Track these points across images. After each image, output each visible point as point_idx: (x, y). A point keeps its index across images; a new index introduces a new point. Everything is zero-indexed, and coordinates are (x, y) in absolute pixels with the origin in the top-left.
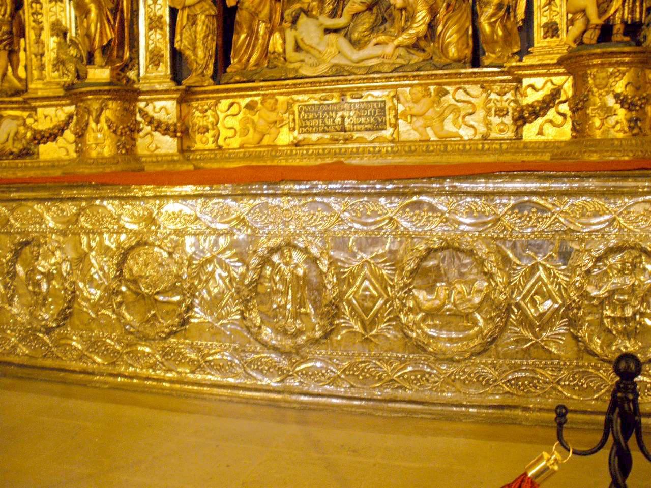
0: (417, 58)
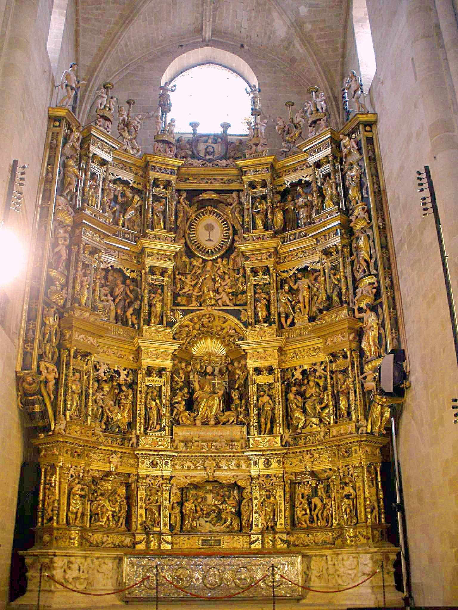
0: (228, 530)
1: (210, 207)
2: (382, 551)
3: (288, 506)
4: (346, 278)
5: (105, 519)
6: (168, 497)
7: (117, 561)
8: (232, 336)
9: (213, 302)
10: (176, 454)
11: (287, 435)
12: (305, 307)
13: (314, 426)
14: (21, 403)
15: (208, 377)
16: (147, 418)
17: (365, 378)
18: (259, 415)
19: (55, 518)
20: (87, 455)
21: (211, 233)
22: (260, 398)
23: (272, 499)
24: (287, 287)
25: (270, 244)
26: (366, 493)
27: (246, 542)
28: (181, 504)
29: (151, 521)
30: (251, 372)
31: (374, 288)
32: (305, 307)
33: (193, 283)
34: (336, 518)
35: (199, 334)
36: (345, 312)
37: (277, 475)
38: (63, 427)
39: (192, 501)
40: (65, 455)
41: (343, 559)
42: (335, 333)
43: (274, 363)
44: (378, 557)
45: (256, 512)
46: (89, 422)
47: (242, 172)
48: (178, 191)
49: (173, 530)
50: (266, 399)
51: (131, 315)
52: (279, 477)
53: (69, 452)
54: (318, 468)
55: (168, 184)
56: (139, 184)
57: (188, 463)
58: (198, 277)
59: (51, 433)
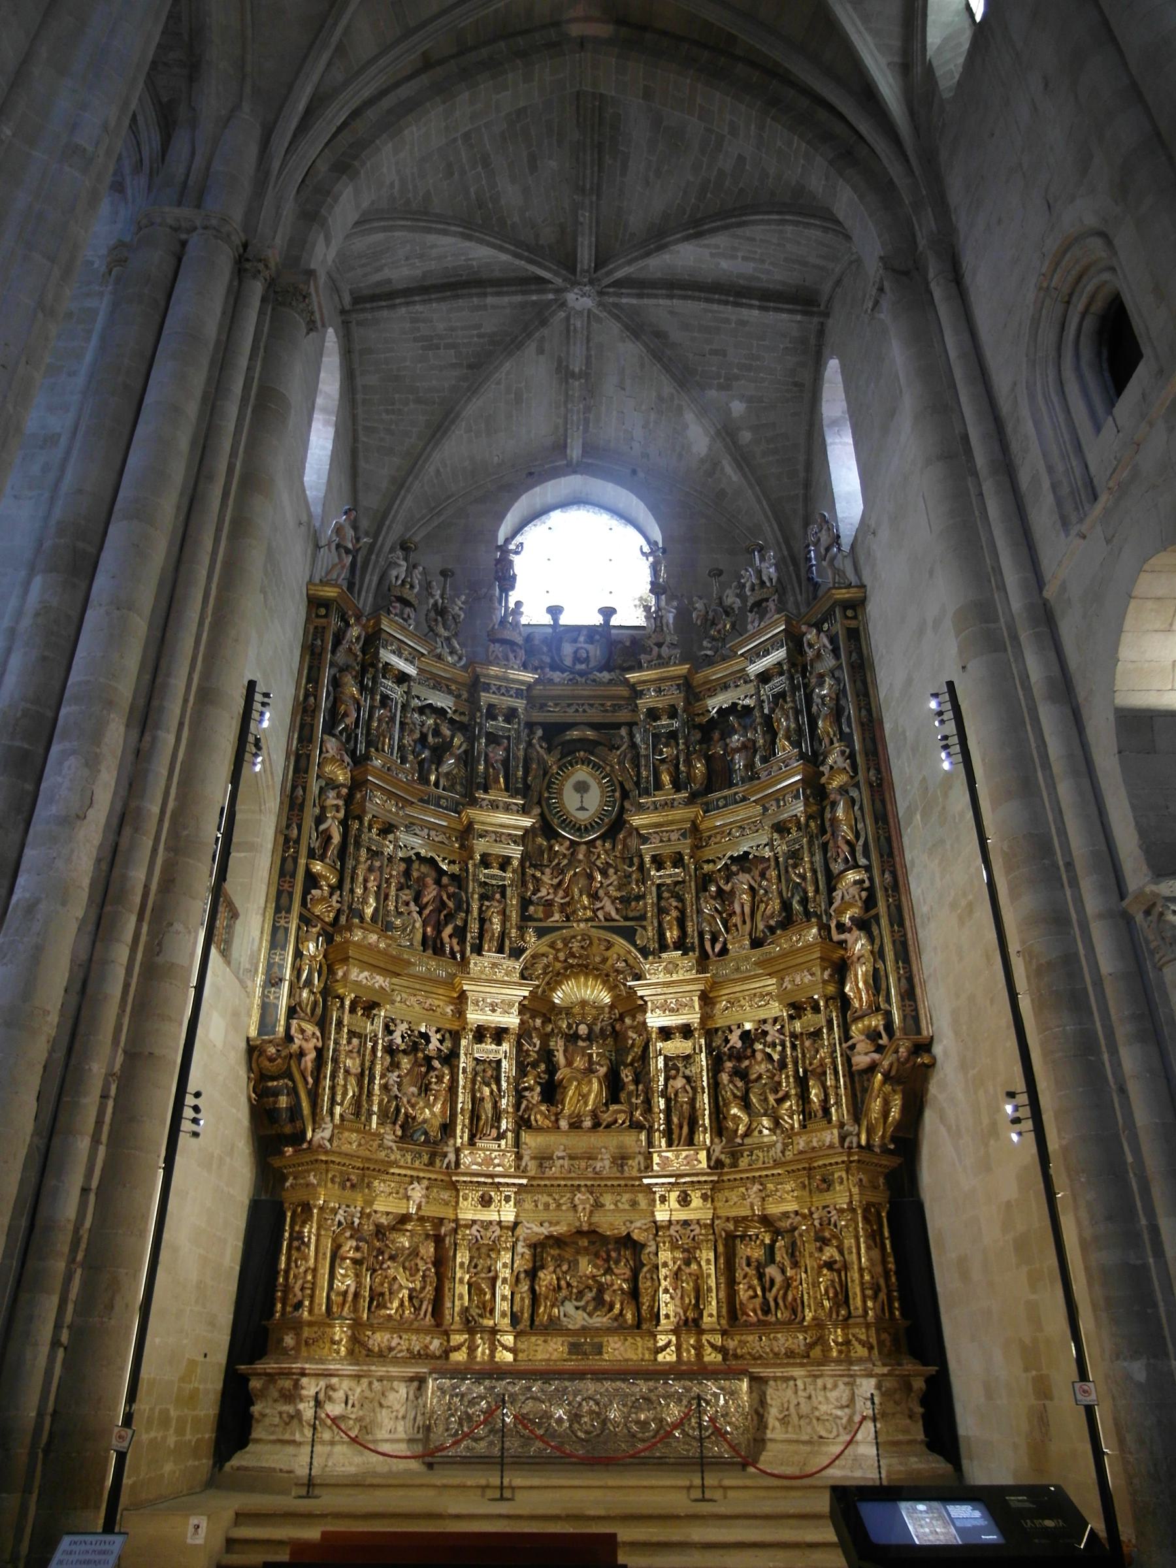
0: (615, 1324)
1: (582, 753)
2: (897, 1372)
3: (722, 1280)
4: (814, 871)
5: (396, 1304)
6: (509, 1261)
7: (416, 1384)
8: (622, 972)
9: (589, 913)
10: (524, 1181)
11: (718, 1149)
12: (744, 922)
13: (766, 1132)
14: (254, 1092)
15: (581, 1043)
16: (475, 1116)
17: (853, 1047)
18: (668, 1111)
19: (307, 1303)
20: (369, 1186)
21: (585, 795)
22: (671, 1082)
23: (694, 1266)
24: (713, 889)
25: (682, 814)
26: (863, 1260)
27: (648, 1349)
28: (532, 1274)
29: (477, 1307)
30: (654, 1036)
31: (863, 889)
32: (744, 922)
33: (555, 881)
34: (809, 1306)
35: (566, 969)
36: (814, 931)
37: (702, 1222)
38: (327, 1134)
39: (551, 1269)
40: (330, 1185)
41: (825, 1388)
42: (798, 967)
43: (693, 1017)
44: (888, 1384)
45: (666, 1291)
46: (374, 1125)
47: (636, 692)
48: (530, 726)
49: (518, 1323)
50: (679, 1083)
51: (450, 936)
52: (706, 1225)
53: (337, 1180)
54: (774, 1209)
55: (511, 714)
56: (463, 714)
57: (545, 1198)
58: (562, 872)
59: (305, 1146)
